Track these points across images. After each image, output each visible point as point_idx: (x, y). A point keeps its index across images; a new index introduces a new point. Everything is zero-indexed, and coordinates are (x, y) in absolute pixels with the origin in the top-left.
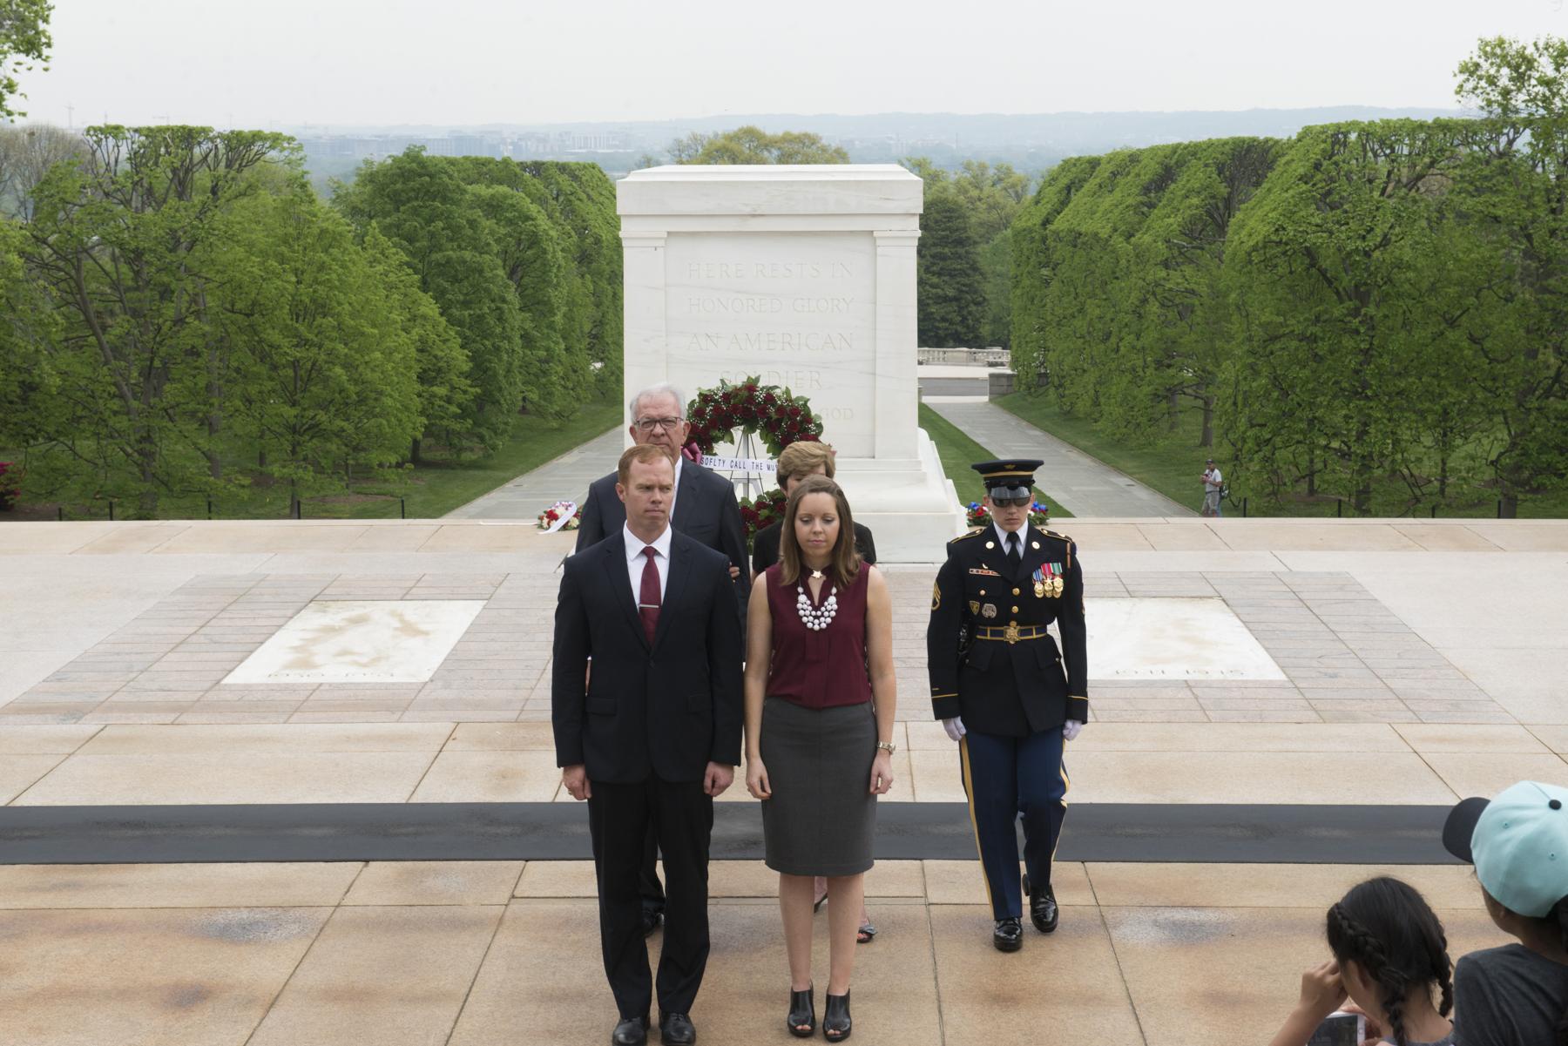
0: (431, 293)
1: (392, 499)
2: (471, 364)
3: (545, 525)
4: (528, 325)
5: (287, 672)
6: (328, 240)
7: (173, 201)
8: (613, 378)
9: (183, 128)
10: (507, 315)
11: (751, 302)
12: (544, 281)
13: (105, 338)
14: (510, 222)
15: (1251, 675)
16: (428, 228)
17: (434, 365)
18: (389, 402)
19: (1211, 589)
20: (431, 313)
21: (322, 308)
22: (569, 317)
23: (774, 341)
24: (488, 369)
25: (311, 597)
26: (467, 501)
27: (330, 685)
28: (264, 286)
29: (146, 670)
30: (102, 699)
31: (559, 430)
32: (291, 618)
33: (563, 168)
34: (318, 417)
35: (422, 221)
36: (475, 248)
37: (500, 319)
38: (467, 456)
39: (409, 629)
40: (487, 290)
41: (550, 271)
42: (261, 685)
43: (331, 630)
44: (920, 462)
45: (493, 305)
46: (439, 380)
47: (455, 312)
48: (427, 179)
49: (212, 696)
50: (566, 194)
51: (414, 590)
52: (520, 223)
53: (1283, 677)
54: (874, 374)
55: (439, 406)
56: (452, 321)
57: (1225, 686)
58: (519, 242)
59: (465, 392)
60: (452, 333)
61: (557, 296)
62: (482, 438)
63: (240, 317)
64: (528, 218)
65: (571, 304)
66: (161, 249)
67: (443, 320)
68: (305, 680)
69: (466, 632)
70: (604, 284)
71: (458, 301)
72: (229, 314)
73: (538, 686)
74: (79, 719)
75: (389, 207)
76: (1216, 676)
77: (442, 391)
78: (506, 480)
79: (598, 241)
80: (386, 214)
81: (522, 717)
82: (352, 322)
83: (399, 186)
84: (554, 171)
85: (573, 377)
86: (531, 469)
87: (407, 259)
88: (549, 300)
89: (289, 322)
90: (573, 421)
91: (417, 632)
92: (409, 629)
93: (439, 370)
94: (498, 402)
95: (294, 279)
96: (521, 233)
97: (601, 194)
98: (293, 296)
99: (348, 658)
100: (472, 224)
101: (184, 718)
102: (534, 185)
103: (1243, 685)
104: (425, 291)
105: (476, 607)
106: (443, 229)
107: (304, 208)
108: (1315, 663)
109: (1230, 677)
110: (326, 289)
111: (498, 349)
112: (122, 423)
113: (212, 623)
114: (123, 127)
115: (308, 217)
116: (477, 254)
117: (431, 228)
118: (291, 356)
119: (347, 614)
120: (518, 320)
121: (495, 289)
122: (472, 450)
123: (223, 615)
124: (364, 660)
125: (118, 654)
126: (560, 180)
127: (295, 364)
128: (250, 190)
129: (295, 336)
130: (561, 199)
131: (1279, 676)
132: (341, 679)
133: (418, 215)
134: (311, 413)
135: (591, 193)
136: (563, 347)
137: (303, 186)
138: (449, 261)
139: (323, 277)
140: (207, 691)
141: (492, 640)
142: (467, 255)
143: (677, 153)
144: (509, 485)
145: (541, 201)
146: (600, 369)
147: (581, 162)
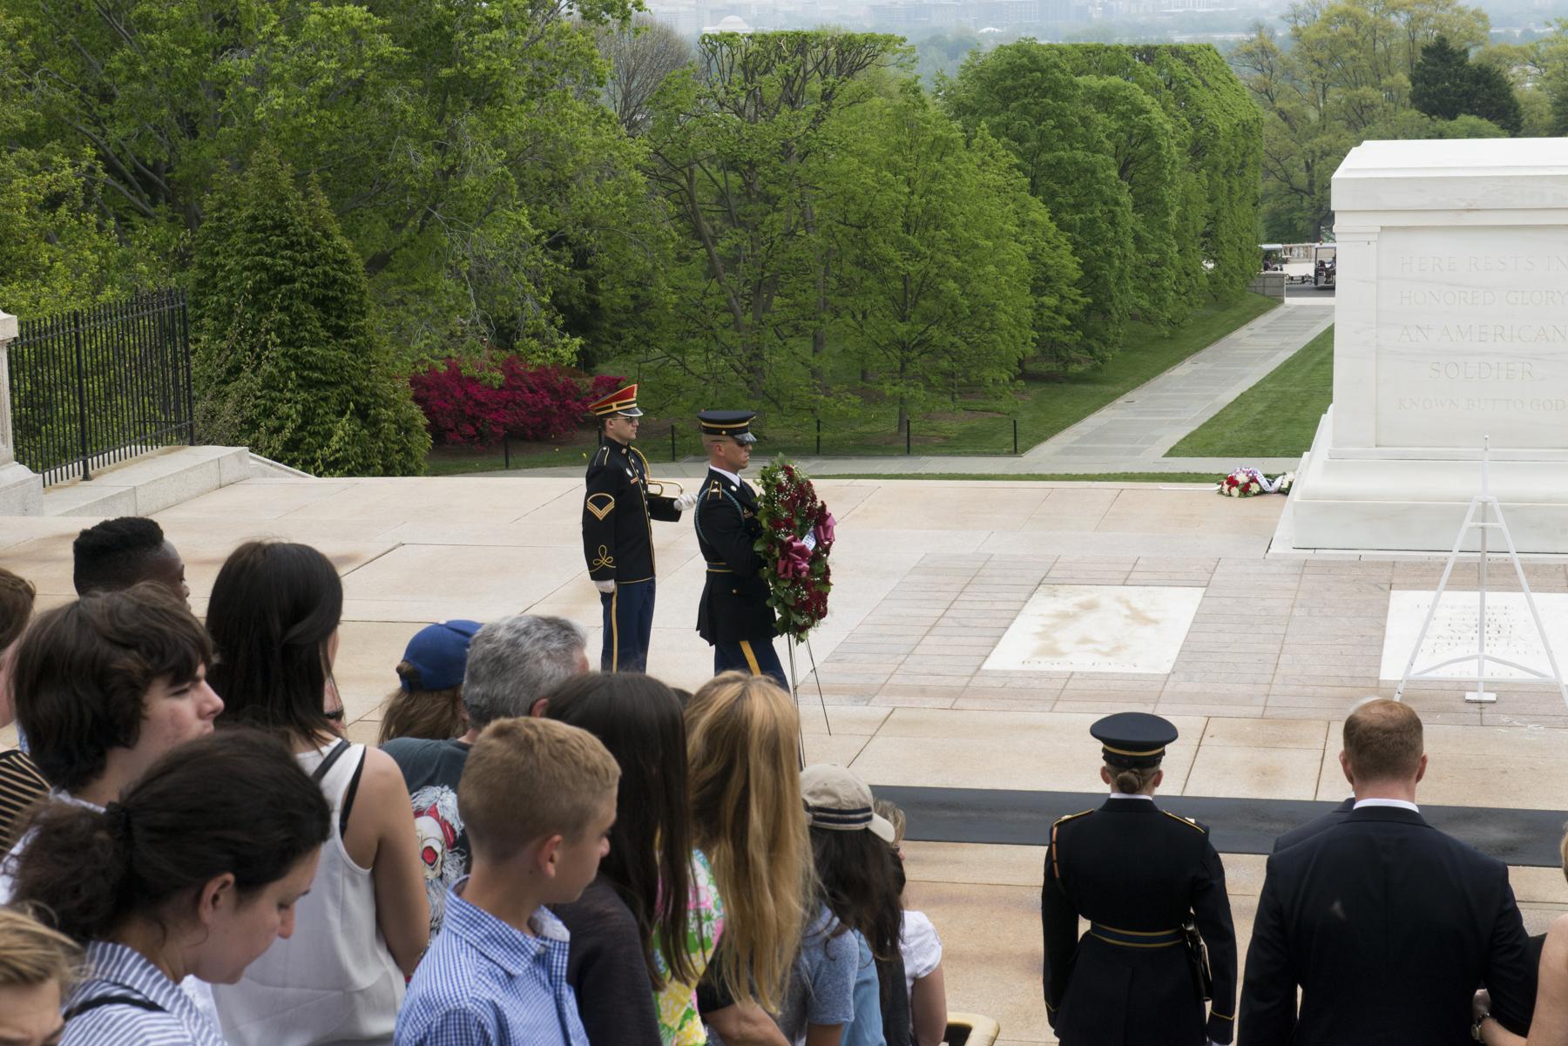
0: (1041, 197)
1: (999, 416)
2: (1081, 273)
3: (1226, 491)
4: (1140, 227)
5: (1038, 659)
6: (942, 147)
7: (785, 110)
8: (1227, 280)
9: (797, 34)
10: (1119, 219)
11: (1463, 295)
12: (1157, 179)
13: (715, 250)
14: (1123, 116)
16: (1038, 128)
17: (1043, 273)
18: (1004, 318)
20: (1040, 218)
21: (934, 219)
22: (1183, 218)
23: (1486, 333)
24: (1098, 276)
25: (1039, 580)
26: (1078, 419)
27: (1082, 674)
28: (878, 197)
30: (883, 681)
31: (1170, 338)
32: (1026, 602)
33: (1176, 51)
34: (929, 332)
35: (1031, 119)
36: (1087, 148)
37: (1112, 223)
38: (1075, 369)
39: (1139, 617)
40: (1099, 192)
41: (1164, 168)
42: (1018, 672)
43: (1065, 616)
45: (1105, 208)
46: (1048, 289)
47: (1066, 217)
48: (1039, 74)
49: (976, 682)
50: (1181, 81)
51: (1132, 576)
52: (1133, 117)
55: (1048, 317)
56: (1062, 226)
58: (1130, 137)
59: (1075, 302)
60: (1063, 240)
61: (1170, 195)
62: (1091, 350)
63: (854, 230)
64: (1141, 111)
65: (1186, 202)
66: (775, 161)
67: (1053, 225)
68: (1056, 668)
69: (1194, 622)
70: (1219, 178)
71: (1069, 205)
72: (842, 226)
73: (1275, 681)
75: (997, 105)
77: (1051, 301)
78: (1116, 396)
79: (1214, 130)
80: (997, 113)
81: (1267, 713)
82: (966, 235)
83: (1009, 83)
84: (1167, 56)
85: (1186, 281)
86: (1143, 383)
87: (1017, 161)
88: (1163, 199)
89: (901, 235)
90: (1183, 328)
92: (1139, 617)
93: (1048, 280)
94: (1109, 311)
95: (907, 190)
96: (1133, 127)
97: (1217, 79)
98: (907, 207)
99: (1089, 646)
100: (1085, 121)
101: (960, 703)
102: (1148, 73)
104: (1034, 193)
105: (1199, 593)
106: (1054, 128)
107: (918, 113)
110: (940, 200)
111: (1109, 254)
112: (727, 336)
113: (956, 603)
114: (738, 34)
115: (922, 124)
116: (1090, 154)
117: (1042, 127)
118: (904, 270)
119: (1076, 600)
120: (1130, 220)
121: (1107, 191)
122: (1079, 363)
123: (962, 597)
124: (1106, 649)
125: (881, 635)
126: (1174, 66)
127: (905, 279)
128: (864, 95)
129: (907, 249)
130: (1174, 86)
132: (1088, 668)
133: (1028, 113)
134: (921, 328)
135: (1206, 78)
136: (1176, 249)
137: (916, 91)
138: (1060, 161)
139: (936, 187)
140: (972, 677)
141: (1220, 631)
142: (1080, 155)
143: (1292, 18)
144: (1120, 401)
145: (1153, 90)
146: (1211, 270)
147: (1196, 44)
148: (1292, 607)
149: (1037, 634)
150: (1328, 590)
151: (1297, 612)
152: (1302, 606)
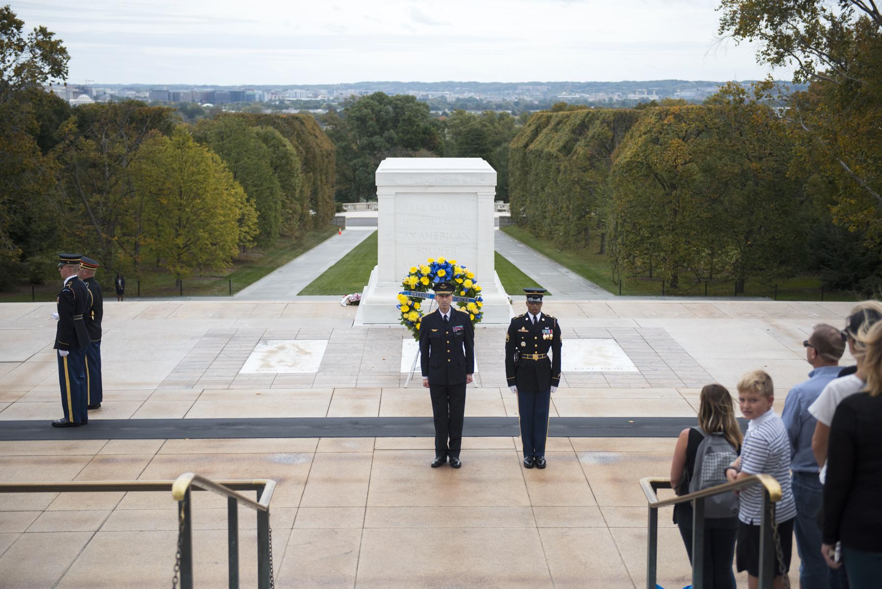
5: (262, 369)
15: (625, 370)
19: (609, 334)
29: (208, 368)
39: (302, 352)
44: (495, 284)
53: (638, 370)
54: (477, 248)
57: (616, 374)
68: (270, 372)
69: (325, 353)
74: (193, 387)
76: (612, 370)
81: (357, 386)
91: (306, 353)
92: (302, 352)
101: (231, 387)
103: (623, 374)
105: (327, 341)
108: (649, 365)
109: (618, 370)
119: (276, 346)
124: (290, 364)
131: (636, 370)
132: (283, 371)
148: (365, 346)
149: (261, 359)
150: (378, 339)
151: (366, 348)
152: (368, 346)
